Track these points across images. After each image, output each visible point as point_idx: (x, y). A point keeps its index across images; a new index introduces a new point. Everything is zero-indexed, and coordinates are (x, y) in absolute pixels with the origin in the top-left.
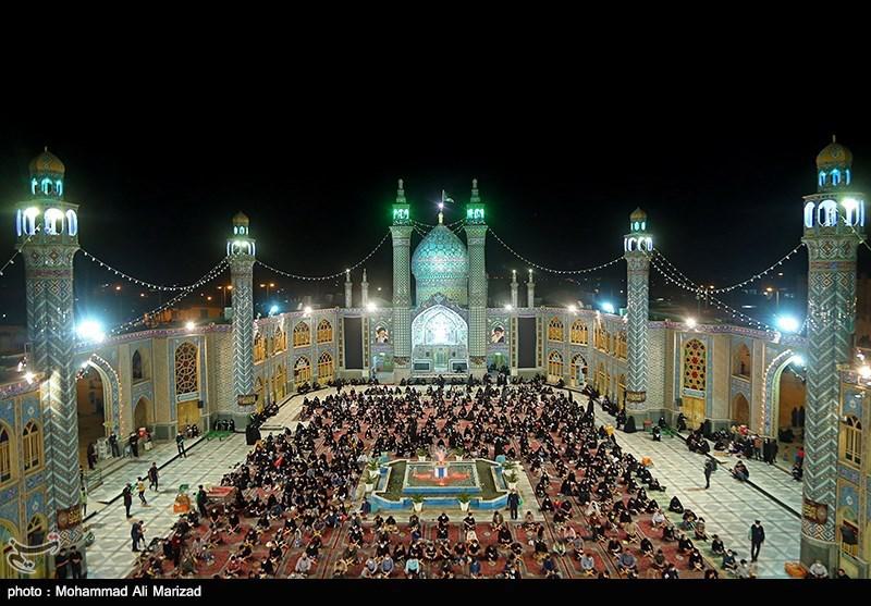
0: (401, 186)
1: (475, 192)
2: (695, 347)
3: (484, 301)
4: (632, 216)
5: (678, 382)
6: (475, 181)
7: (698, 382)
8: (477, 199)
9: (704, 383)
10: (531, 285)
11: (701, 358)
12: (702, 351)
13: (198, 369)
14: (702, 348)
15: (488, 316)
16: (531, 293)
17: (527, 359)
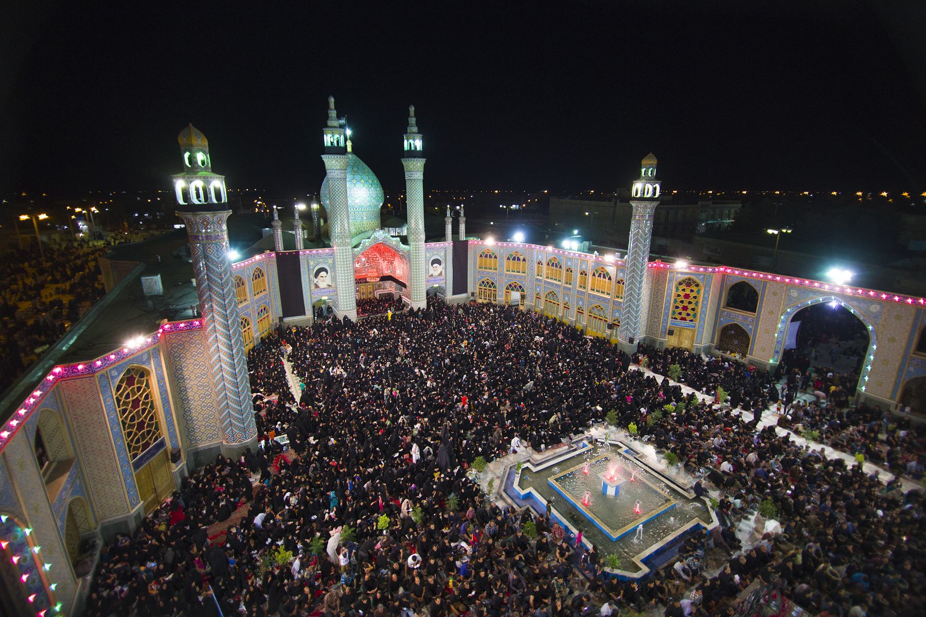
0: (332, 105)
1: (413, 120)
2: (688, 285)
3: (423, 237)
4: (644, 162)
5: (667, 315)
6: (412, 109)
7: (688, 315)
8: (415, 129)
9: (695, 315)
10: (462, 220)
11: (692, 295)
12: (695, 289)
13: (158, 402)
14: (697, 285)
15: (427, 249)
16: (462, 227)
17: (460, 285)
